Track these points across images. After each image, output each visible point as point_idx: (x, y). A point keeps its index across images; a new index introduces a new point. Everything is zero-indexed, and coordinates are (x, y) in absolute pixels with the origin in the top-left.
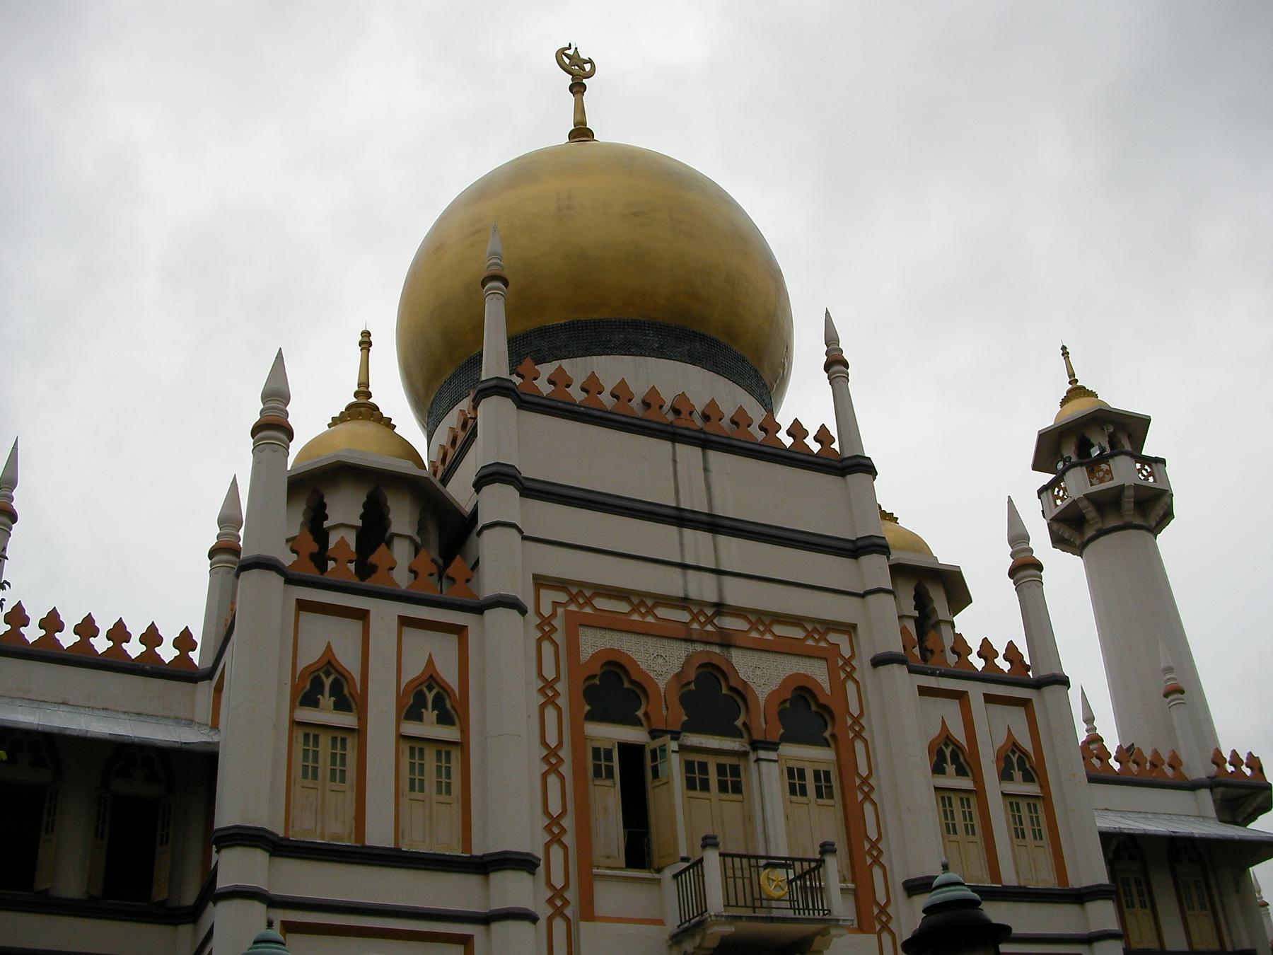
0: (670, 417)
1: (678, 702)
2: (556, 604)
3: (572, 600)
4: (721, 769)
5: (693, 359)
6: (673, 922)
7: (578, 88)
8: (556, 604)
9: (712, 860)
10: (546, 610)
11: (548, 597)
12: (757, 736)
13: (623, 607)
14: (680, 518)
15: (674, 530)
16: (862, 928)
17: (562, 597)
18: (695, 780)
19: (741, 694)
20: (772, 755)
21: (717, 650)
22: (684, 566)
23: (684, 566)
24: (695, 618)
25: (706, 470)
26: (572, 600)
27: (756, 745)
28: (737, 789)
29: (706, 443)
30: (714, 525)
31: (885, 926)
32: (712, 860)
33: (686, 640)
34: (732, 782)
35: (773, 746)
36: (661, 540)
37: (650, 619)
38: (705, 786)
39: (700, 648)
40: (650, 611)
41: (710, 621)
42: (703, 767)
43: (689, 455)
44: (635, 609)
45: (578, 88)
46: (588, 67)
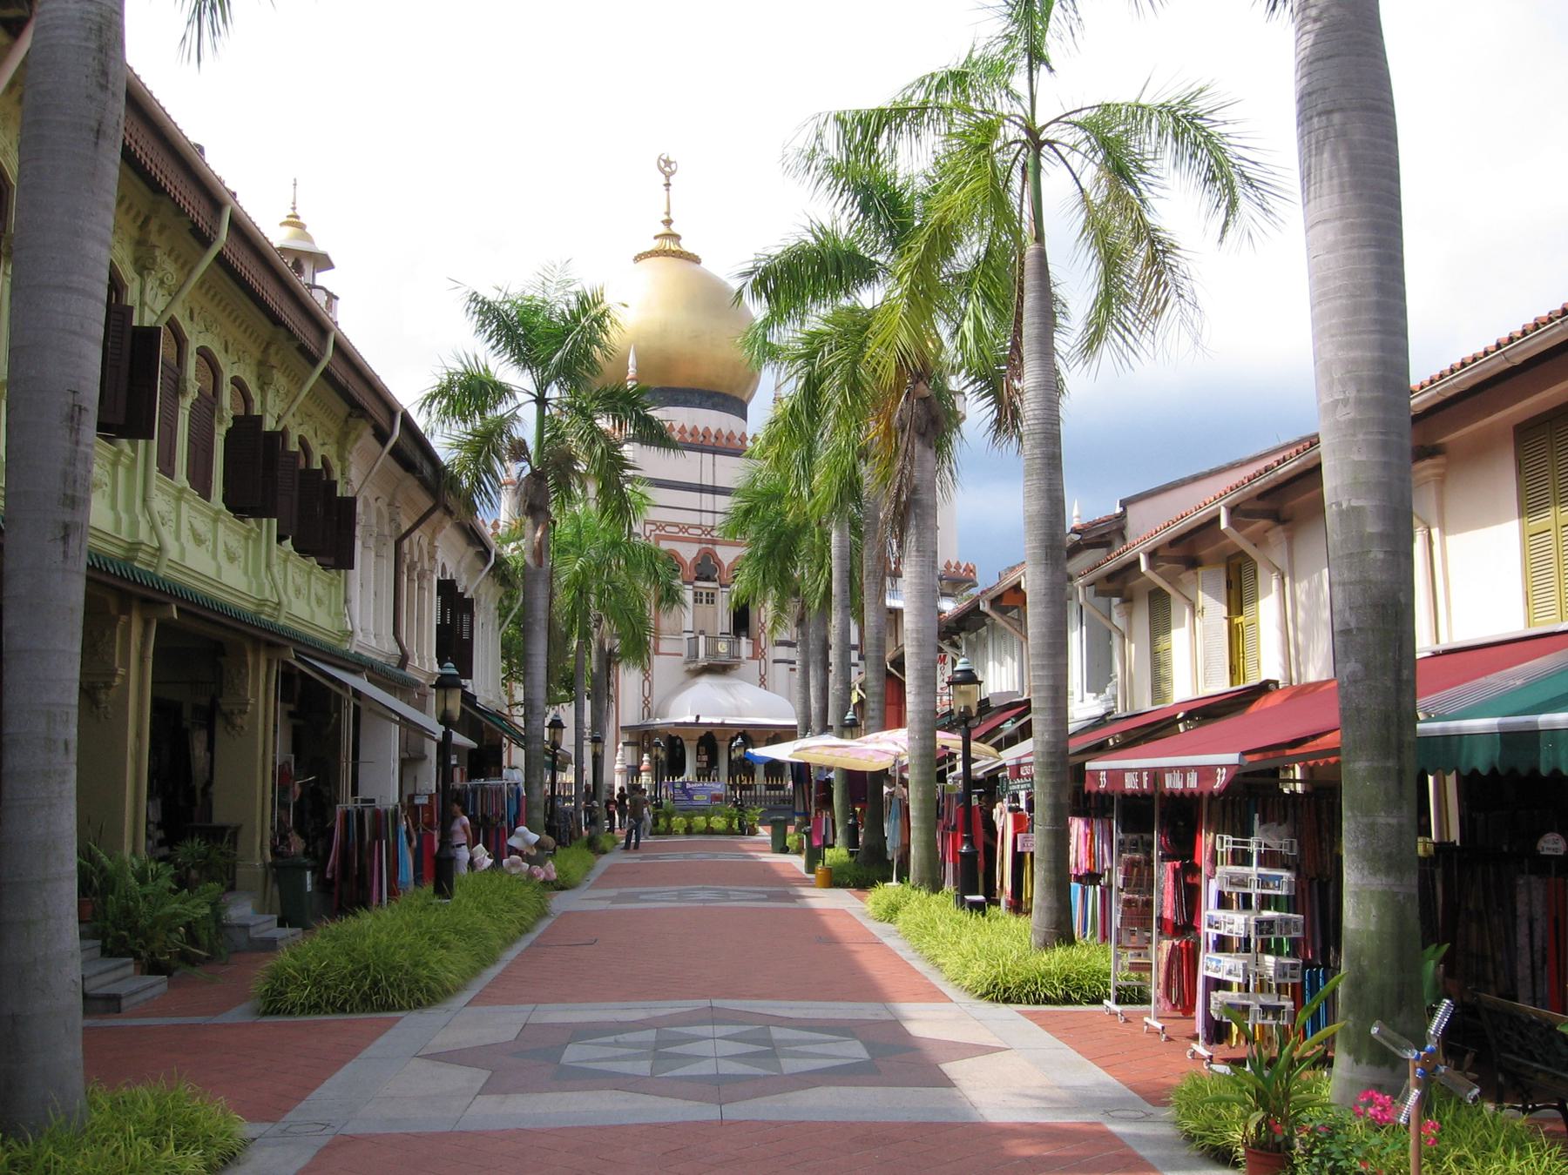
0: (701, 438)
1: (693, 569)
2: (651, 531)
3: (658, 528)
4: (707, 594)
5: (714, 407)
6: (686, 654)
7: (668, 185)
8: (651, 531)
9: (702, 638)
10: (648, 534)
11: (649, 527)
12: (723, 582)
13: (677, 530)
14: (701, 489)
15: (698, 494)
16: (753, 658)
17: (654, 527)
18: (697, 599)
19: (719, 563)
20: (728, 590)
21: (710, 546)
22: (701, 511)
23: (701, 511)
24: (703, 532)
25: (714, 465)
26: (658, 528)
27: (721, 586)
28: (713, 602)
29: (715, 451)
30: (714, 490)
31: (763, 657)
32: (702, 638)
33: (700, 543)
34: (711, 598)
35: (728, 586)
36: (692, 499)
37: (686, 535)
38: (701, 601)
39: (704, 546)
40: (686, 531)
41: (709, 533)
42: (701, 594)
43: (708, 457)
44: (681, 530)
45: (668, 185)
46: (673, 166)
